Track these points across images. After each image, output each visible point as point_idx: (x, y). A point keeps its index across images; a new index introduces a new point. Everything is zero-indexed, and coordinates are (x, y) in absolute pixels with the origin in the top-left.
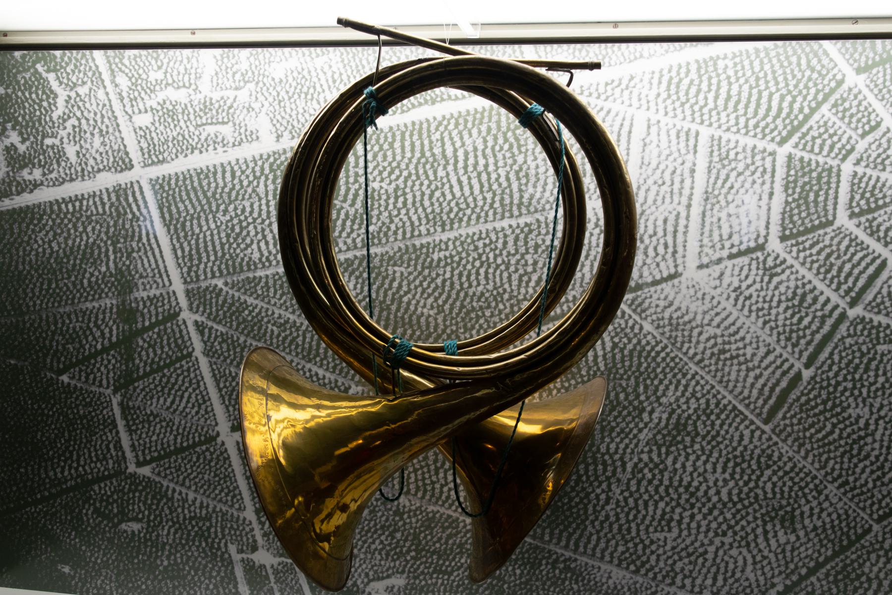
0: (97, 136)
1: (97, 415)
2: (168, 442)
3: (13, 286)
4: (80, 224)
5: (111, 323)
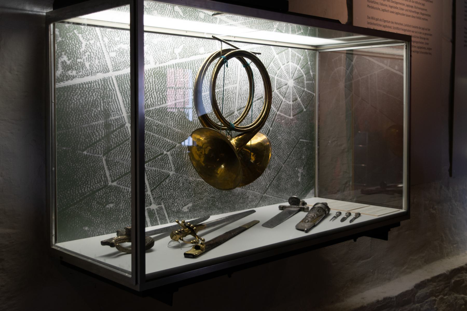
0: (97, 59)
1: (97, 165)
2: (122, 172)
3: (65, 117)
4: (90, 93)
5: (102, 129)
